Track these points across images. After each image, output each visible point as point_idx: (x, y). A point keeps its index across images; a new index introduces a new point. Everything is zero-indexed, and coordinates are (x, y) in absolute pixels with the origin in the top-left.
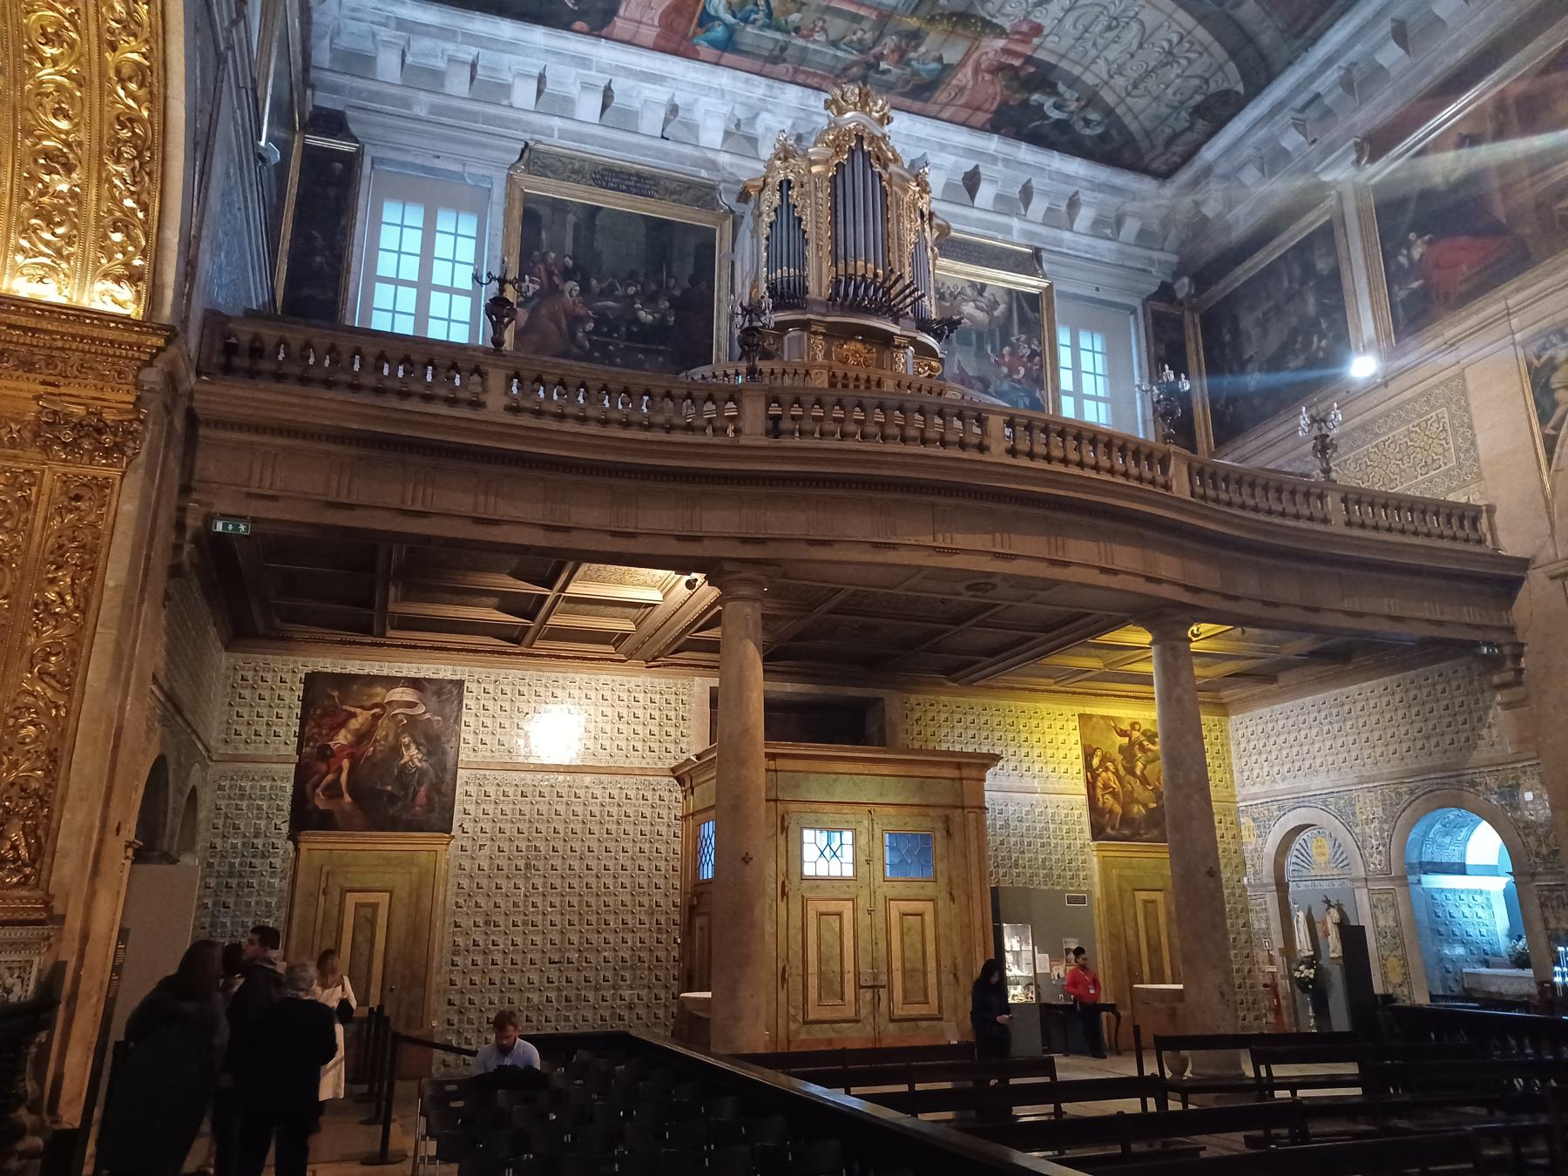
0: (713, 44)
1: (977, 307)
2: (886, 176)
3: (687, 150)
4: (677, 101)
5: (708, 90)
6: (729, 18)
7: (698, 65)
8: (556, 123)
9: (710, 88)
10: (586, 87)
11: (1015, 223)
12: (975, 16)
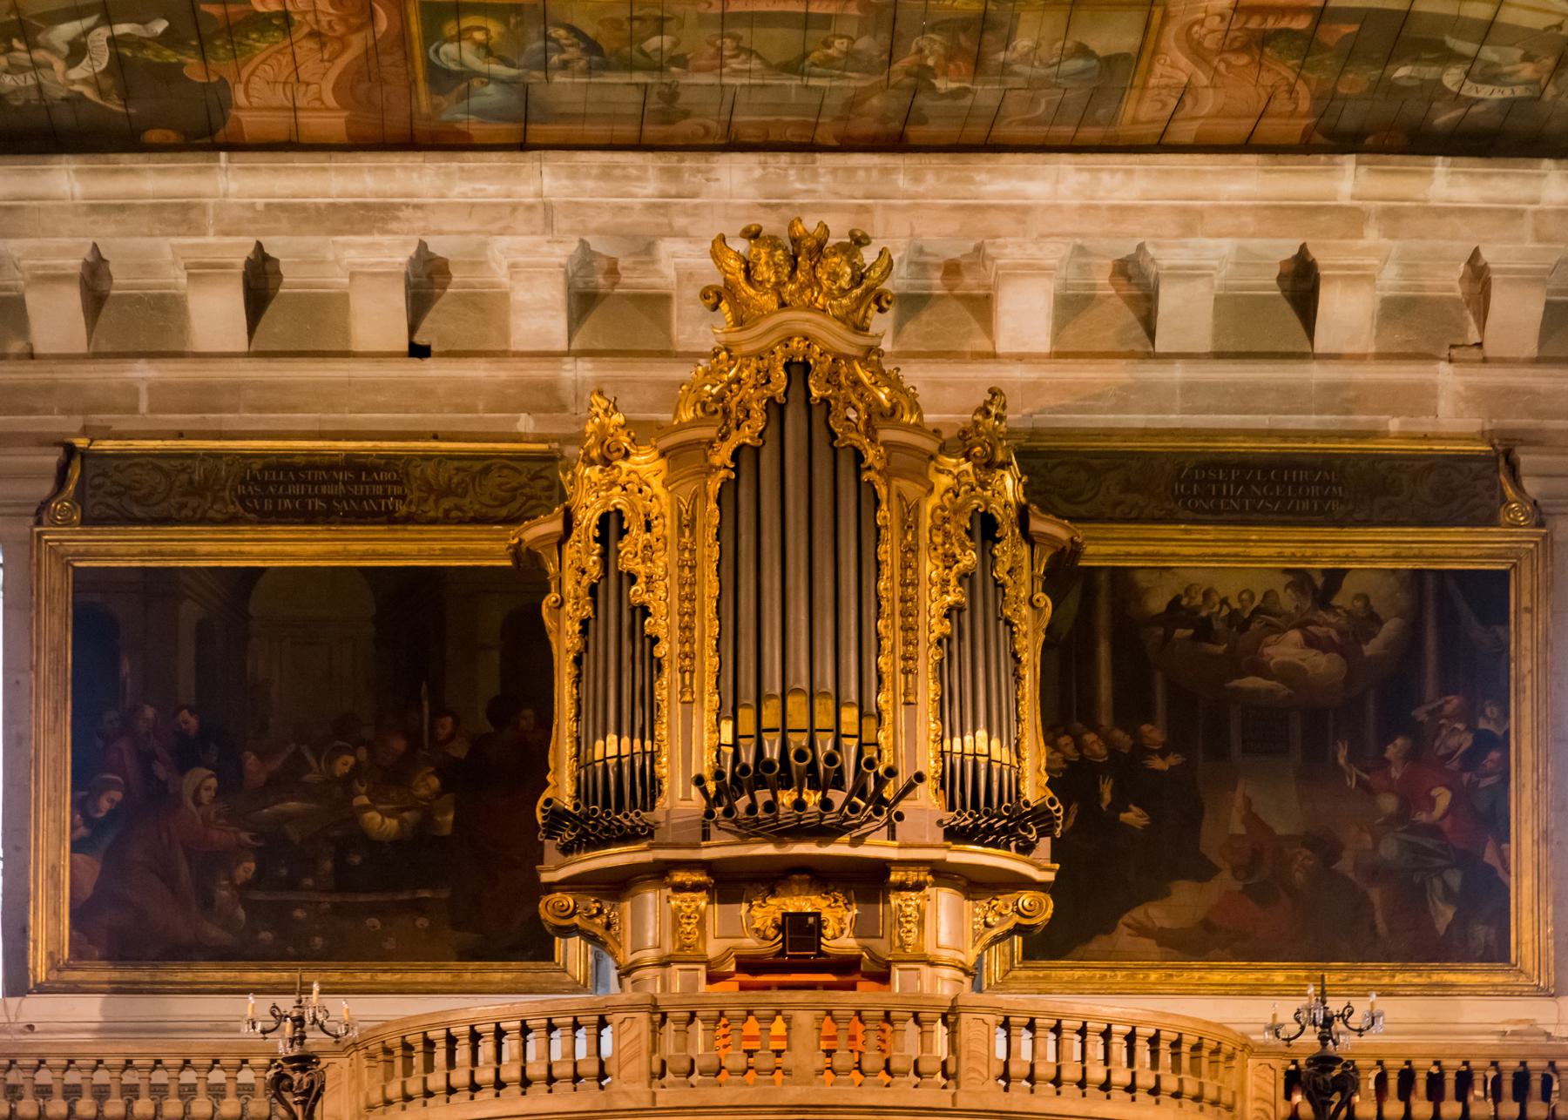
2: (871, 455)
3: (477, 371)
4: (437, 246)
5: (505, 215)
7: (472, 161)
8: (142, 372)
9: (514, 208)
10: (201, 272)
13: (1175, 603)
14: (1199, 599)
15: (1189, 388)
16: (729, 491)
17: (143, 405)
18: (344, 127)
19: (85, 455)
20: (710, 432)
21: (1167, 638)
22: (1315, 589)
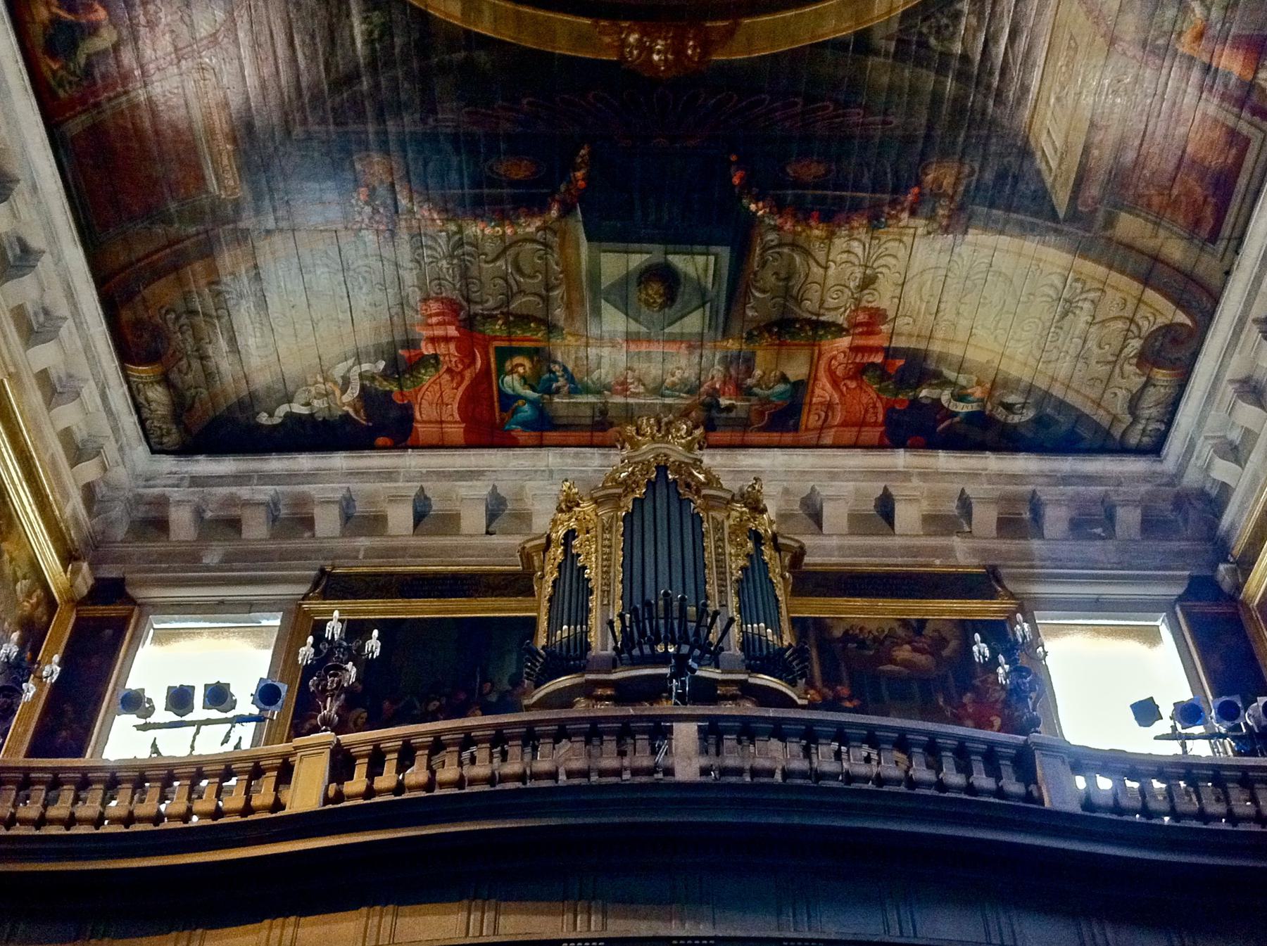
0: (526, 425)
1: (915, 650)
4: (502, 492)
5: (533, 473)
6: (529, 393)
7: (518, 451)
8: (363, 542)
9: (536, 471)
10: (395, 499)
11: (956, 542)
12: (797, 320)
13: (846, 632)
14: (858, 631)
15: (840, 548)
16: (628, 519)
17: (361, 557)
18: (462, 435)
19: (330, 575)
20: (620, 491)
21: (844, 648)
22: (913, 628)
